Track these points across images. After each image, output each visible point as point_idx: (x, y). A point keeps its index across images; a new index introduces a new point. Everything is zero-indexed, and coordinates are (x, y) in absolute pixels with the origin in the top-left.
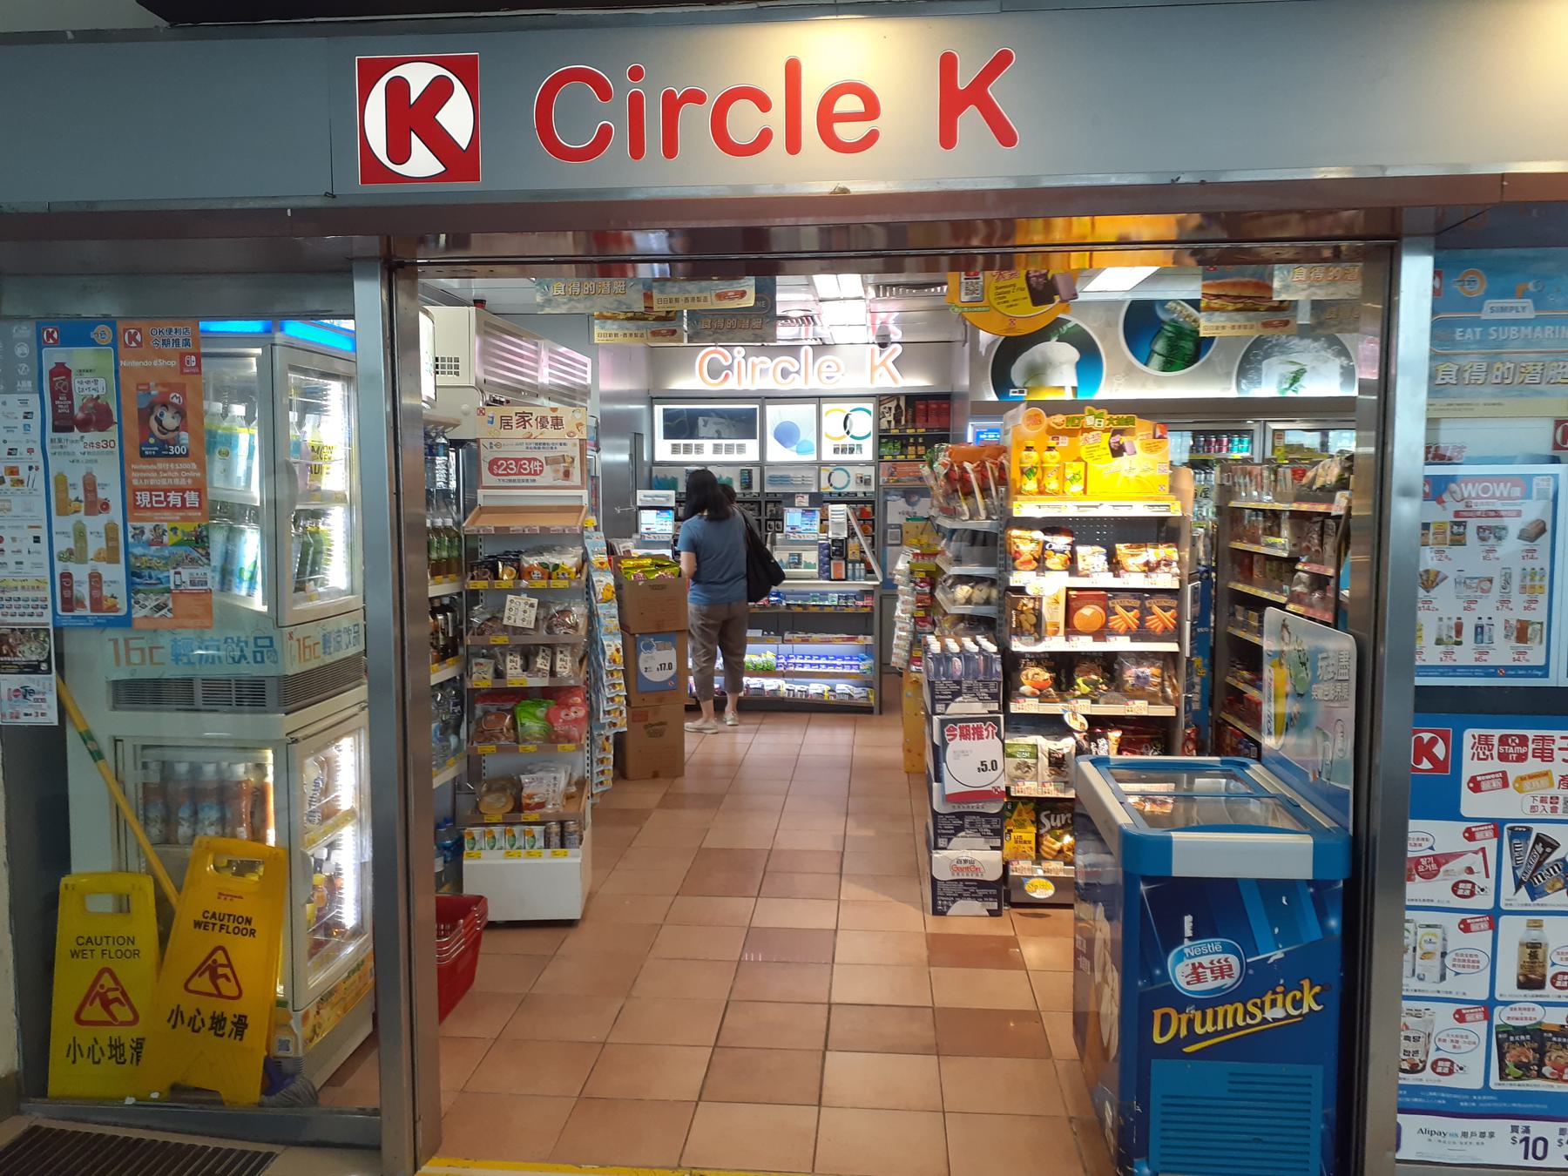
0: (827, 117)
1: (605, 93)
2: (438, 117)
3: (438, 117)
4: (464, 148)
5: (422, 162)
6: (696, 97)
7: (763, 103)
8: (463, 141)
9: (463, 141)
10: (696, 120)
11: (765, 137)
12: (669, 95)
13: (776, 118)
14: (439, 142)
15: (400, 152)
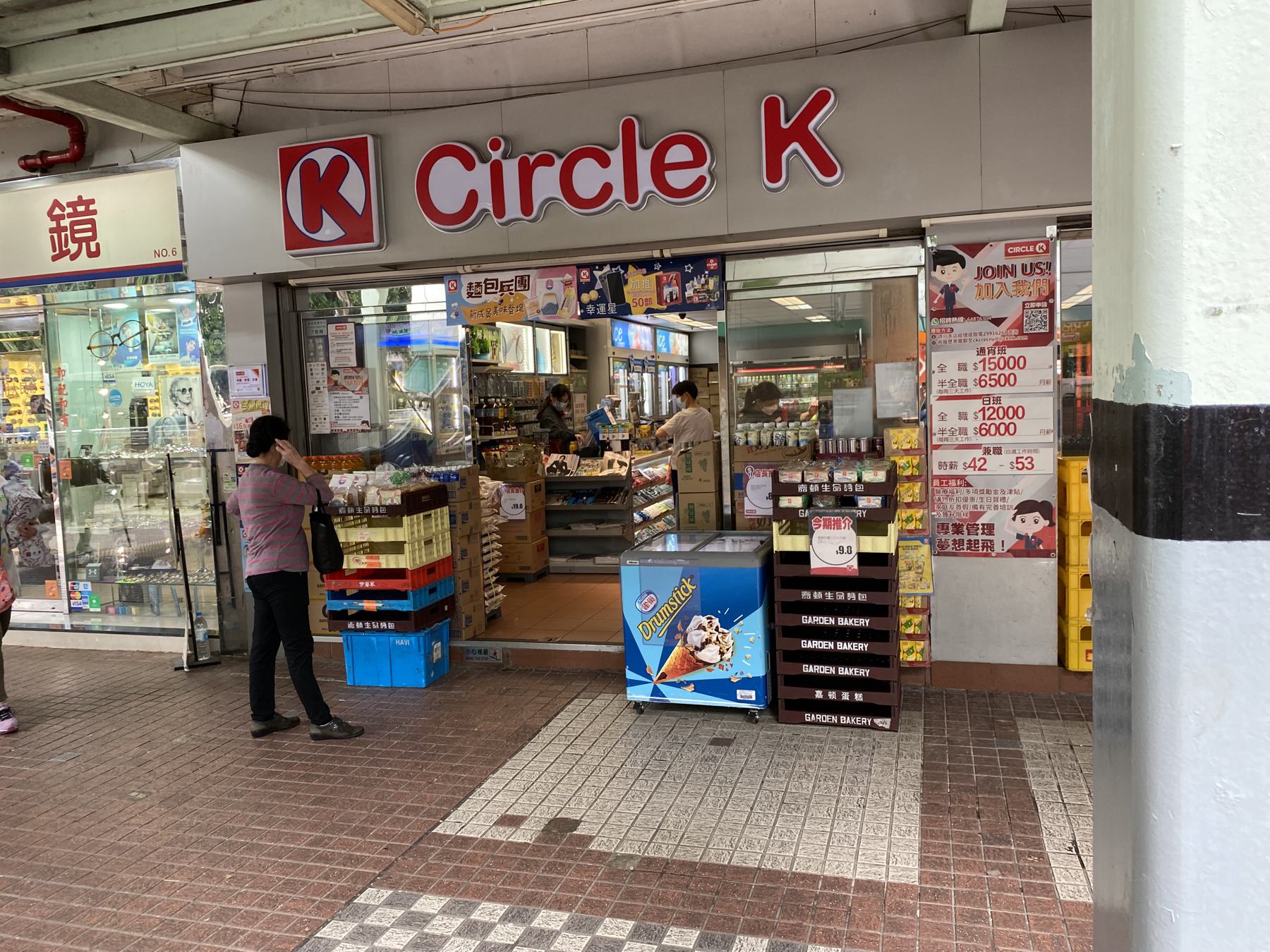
0: (659, 169)
1: (469, 165)
2: (340, 191)
3: (340, 191)
4: (360, 213)
5: (330, 229)
6: (547, 161)
7: (605, 162)
8: (359, 207)
9: (359, 208)
10: (546, 181)
11: (607, 189)
12: (523, 163)
13: (615, 174)
14: (341, 210)
15: (314, 223)
